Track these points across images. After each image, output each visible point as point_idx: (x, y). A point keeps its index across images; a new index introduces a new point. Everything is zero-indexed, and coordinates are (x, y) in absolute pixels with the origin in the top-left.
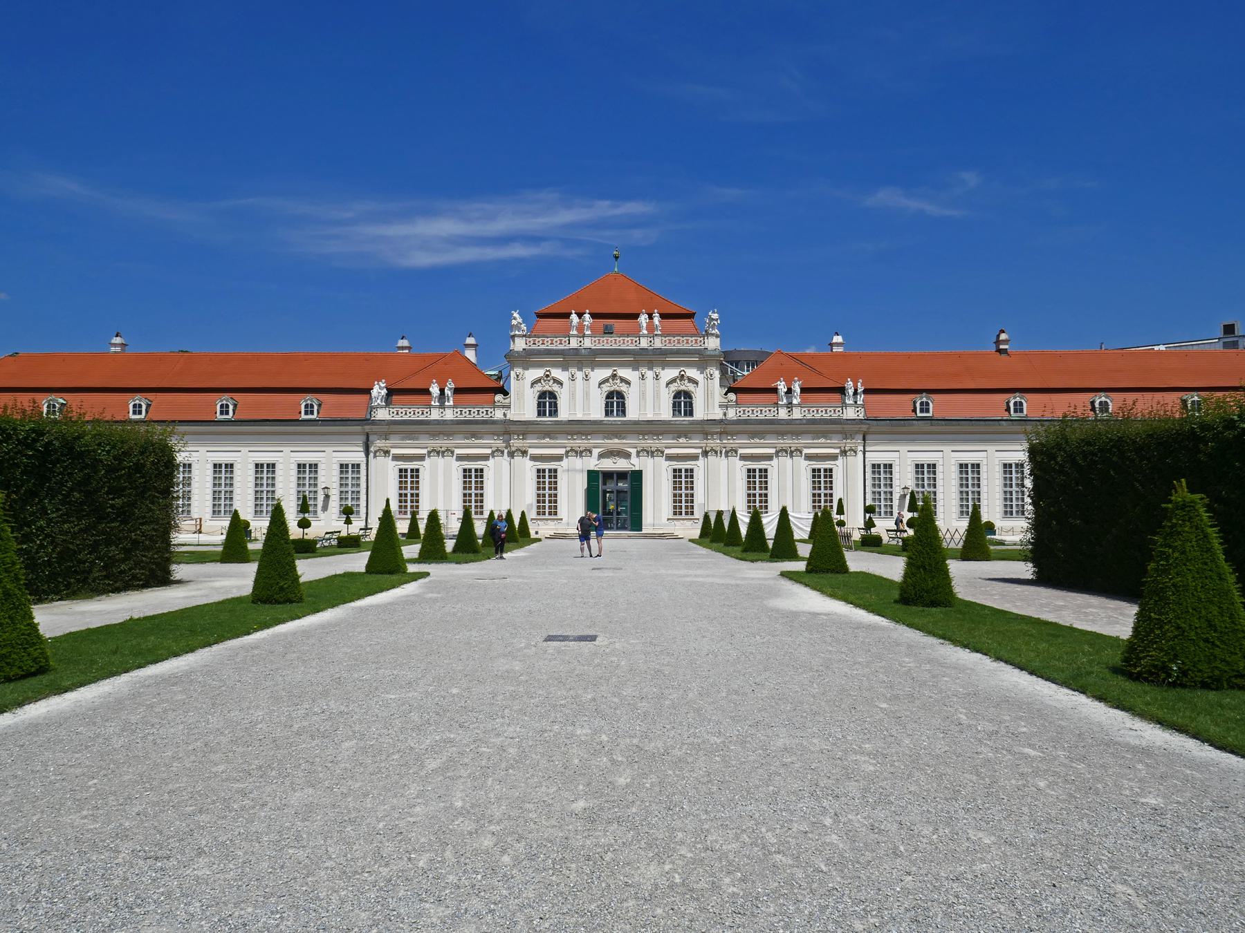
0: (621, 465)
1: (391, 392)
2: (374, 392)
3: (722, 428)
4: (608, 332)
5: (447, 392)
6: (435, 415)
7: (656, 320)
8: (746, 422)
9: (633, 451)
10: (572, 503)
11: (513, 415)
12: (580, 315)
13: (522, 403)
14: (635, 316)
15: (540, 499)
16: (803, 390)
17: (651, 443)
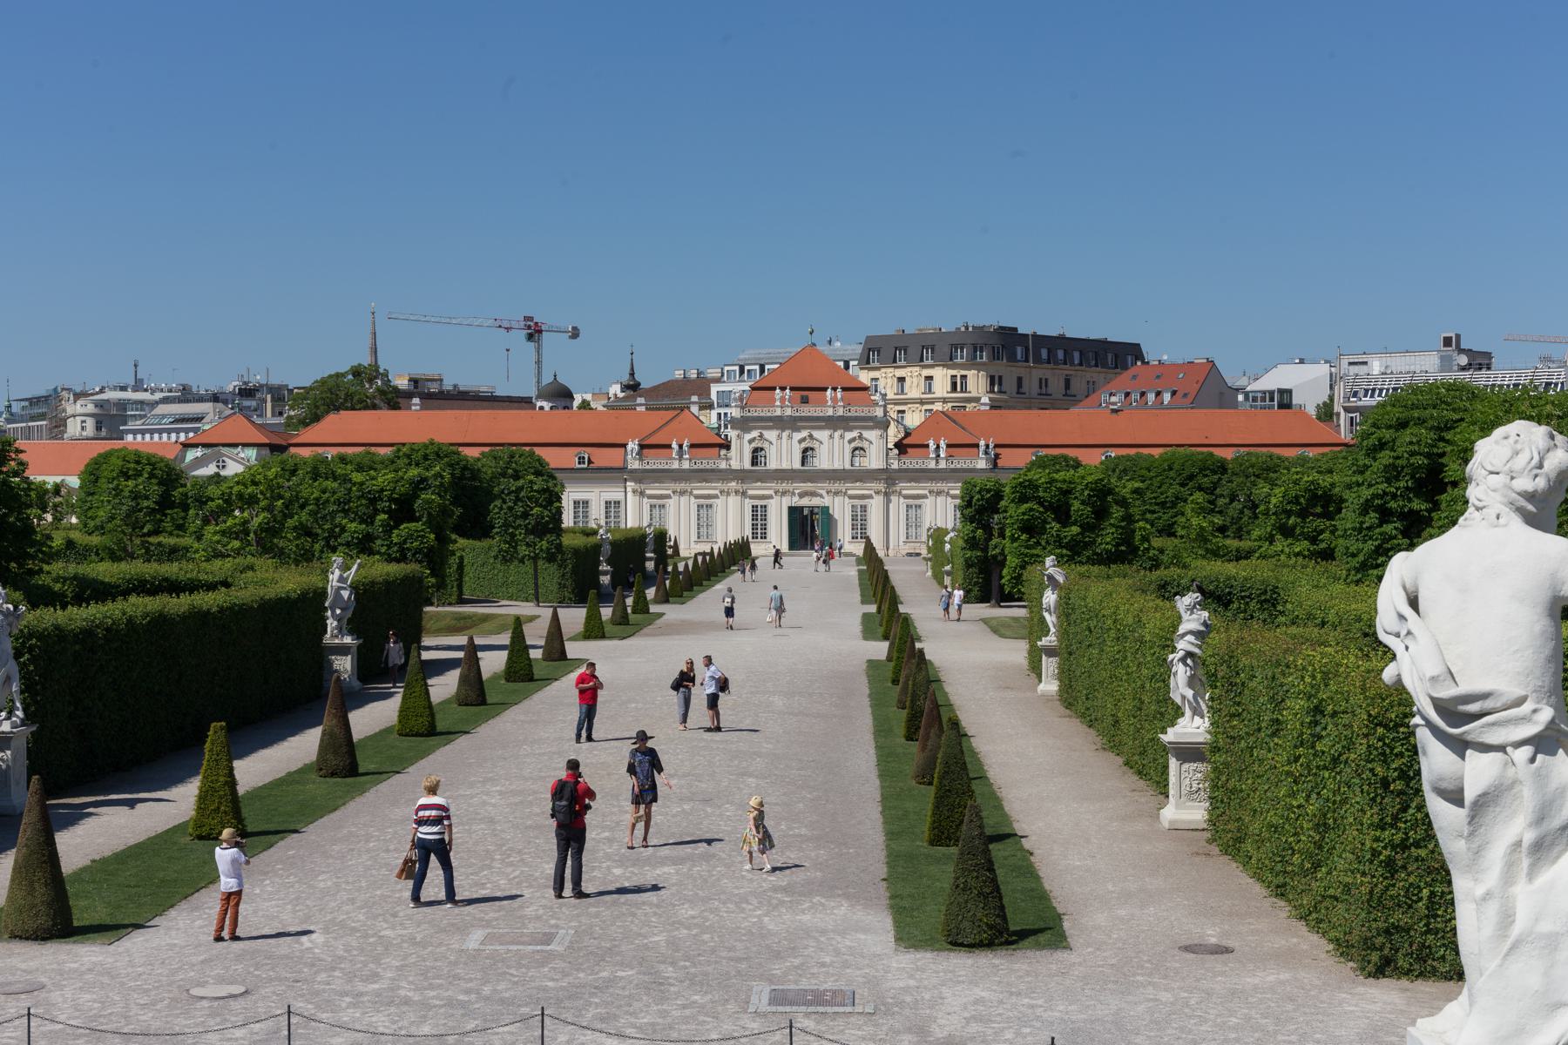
0: (816, 501)
1: (642, 447)
2: (629, 447)
3: (889, 478)
4: (805, 401)
5: (685, 448)
6: (676, 465)
7: (839, 394)
8: (906, 470)
9: (823, 492)
10: (778, 532)
11: (735, 465)
12: (783, 389)
13: (739, 458)
14: (825, 389)
15: (754, 527)
16: (948, 446)
17: (837, 486)
